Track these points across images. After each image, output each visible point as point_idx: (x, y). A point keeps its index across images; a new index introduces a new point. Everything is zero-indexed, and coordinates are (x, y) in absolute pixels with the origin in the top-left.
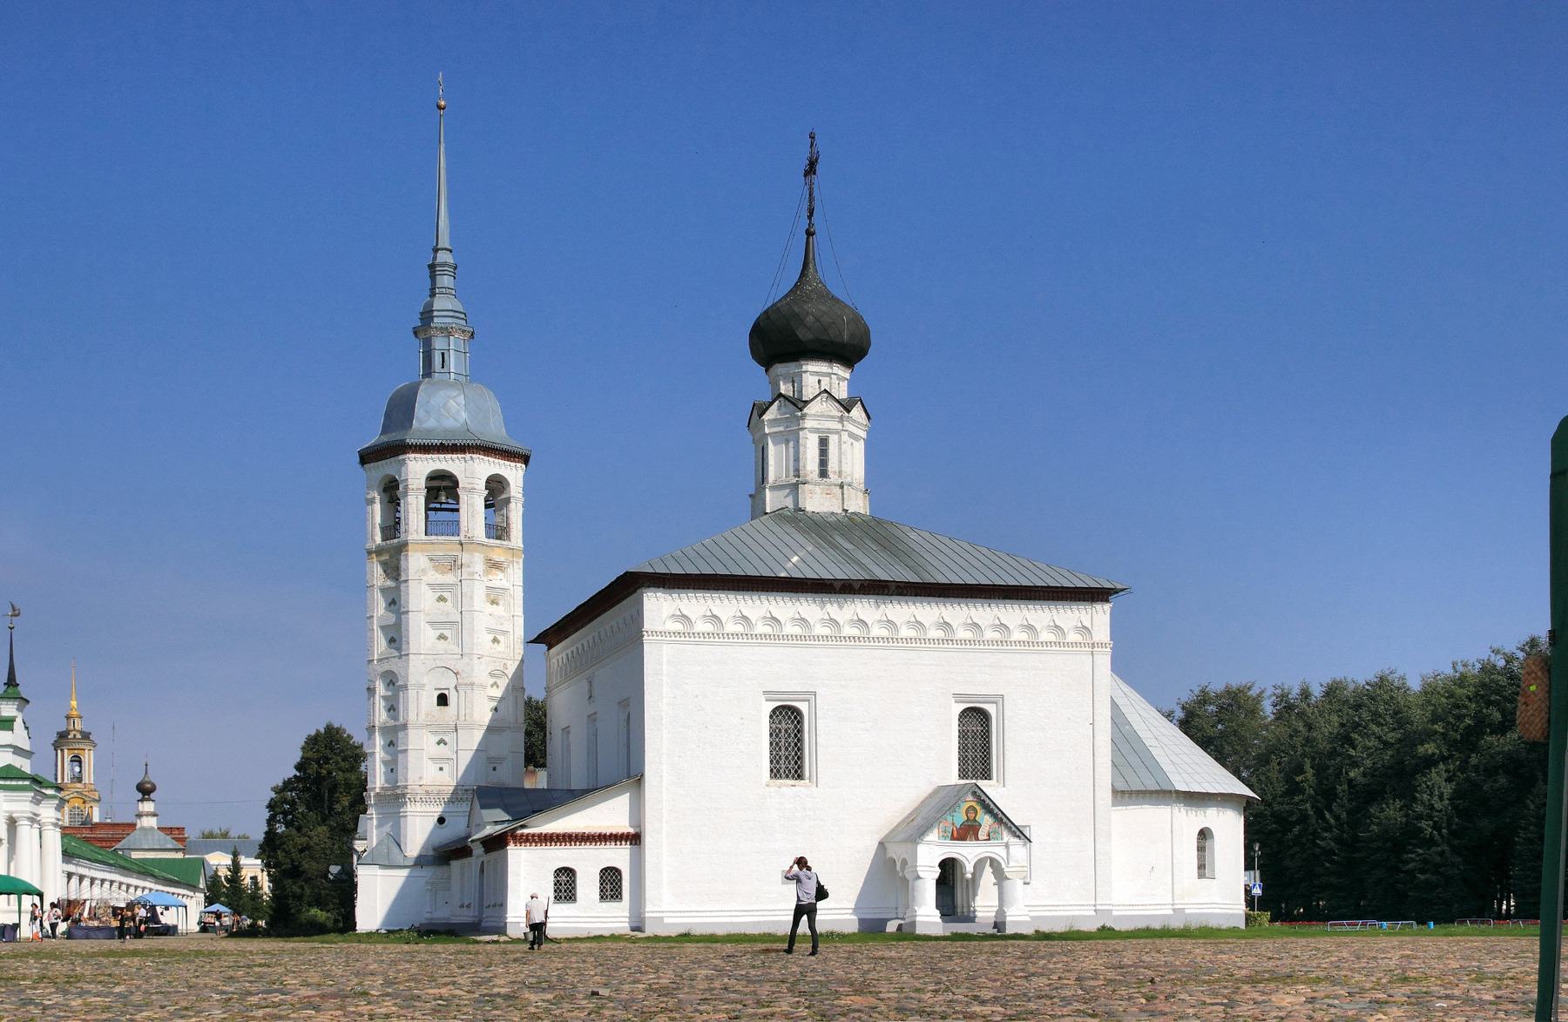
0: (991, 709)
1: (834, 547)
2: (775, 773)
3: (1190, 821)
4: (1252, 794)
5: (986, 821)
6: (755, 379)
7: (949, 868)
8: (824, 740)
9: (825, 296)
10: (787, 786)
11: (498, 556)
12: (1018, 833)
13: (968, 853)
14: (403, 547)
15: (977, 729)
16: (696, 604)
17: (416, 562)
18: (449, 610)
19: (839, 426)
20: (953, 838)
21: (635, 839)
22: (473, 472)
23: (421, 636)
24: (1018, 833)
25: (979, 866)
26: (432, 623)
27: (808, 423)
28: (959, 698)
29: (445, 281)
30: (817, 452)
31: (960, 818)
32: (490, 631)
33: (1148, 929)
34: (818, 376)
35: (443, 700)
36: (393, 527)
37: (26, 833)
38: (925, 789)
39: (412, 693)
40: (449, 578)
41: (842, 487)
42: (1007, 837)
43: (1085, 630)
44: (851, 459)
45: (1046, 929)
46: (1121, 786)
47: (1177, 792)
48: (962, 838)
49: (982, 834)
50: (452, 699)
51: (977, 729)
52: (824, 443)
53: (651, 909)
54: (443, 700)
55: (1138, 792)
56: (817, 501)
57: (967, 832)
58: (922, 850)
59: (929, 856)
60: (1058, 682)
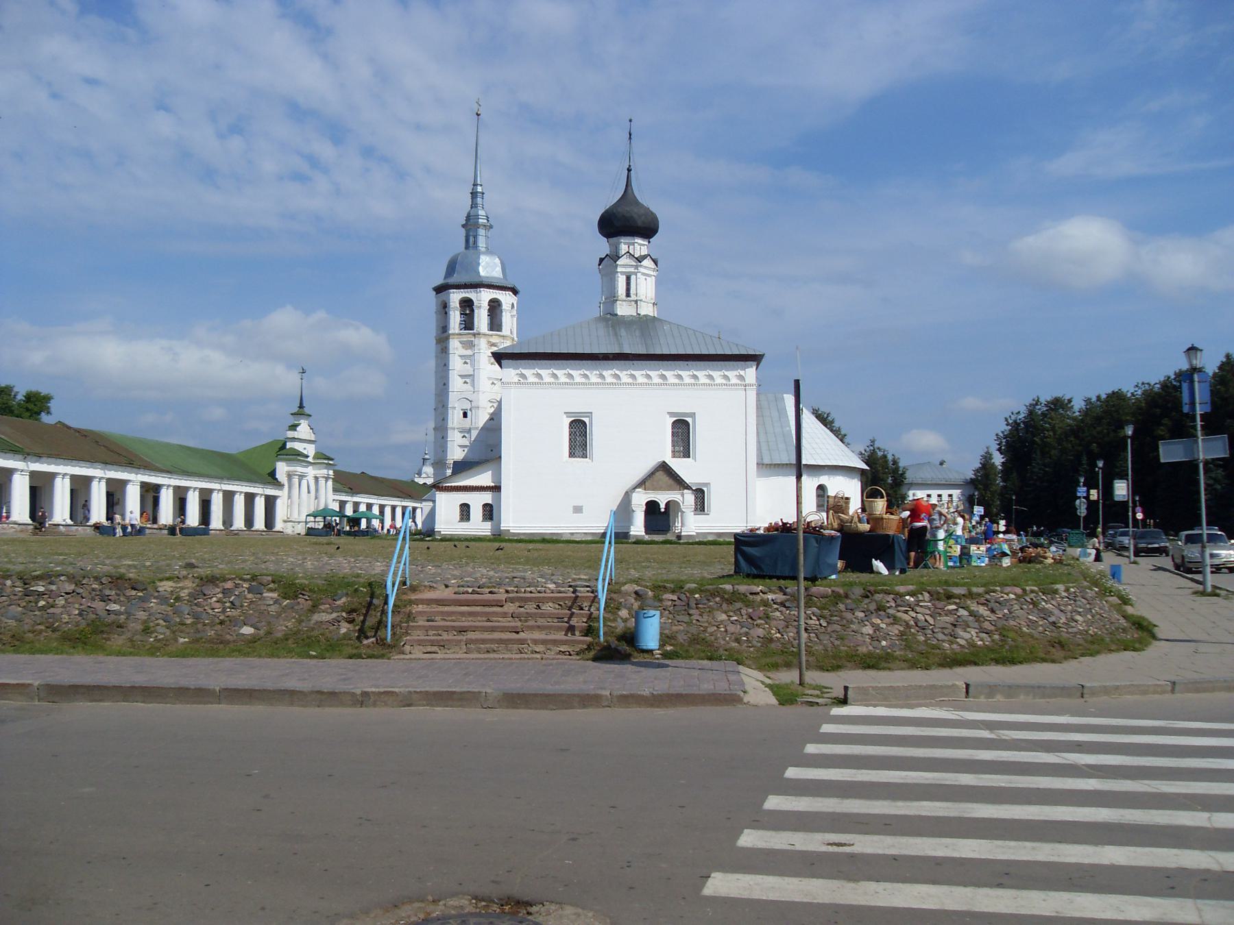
0: (689, 420)
1: (616, 334)
2: (572, 455)
4: (866, 467)
6: (603, 246)
7: (652, 507)
8: (597, 436)
9: (637, 203)
13: (662, 498)
14: (447, 338)
15: (682, 431)
17: (455, 345)
18: (468, 369)
21: (496, 489)
22: (483, 298)
23: (456, 384)
25: (668, 504)
27: (619, 269)
28: (671, 414)
29: (479, 200)
32: (489, 378)
34: (640, 246)
36: (444, 328)
37: (322, 482)
39: (450, 411)
40: (469, 352)
41: (636, 302)
43: (741, 378)
44: (646, 286)
46: (767, 461)
50: (469, 414)
51: (682, 431)
53: (504, 526)
54: (465, 415)
56: (623, 309)
59: (640, 500)
60: (725, 408)
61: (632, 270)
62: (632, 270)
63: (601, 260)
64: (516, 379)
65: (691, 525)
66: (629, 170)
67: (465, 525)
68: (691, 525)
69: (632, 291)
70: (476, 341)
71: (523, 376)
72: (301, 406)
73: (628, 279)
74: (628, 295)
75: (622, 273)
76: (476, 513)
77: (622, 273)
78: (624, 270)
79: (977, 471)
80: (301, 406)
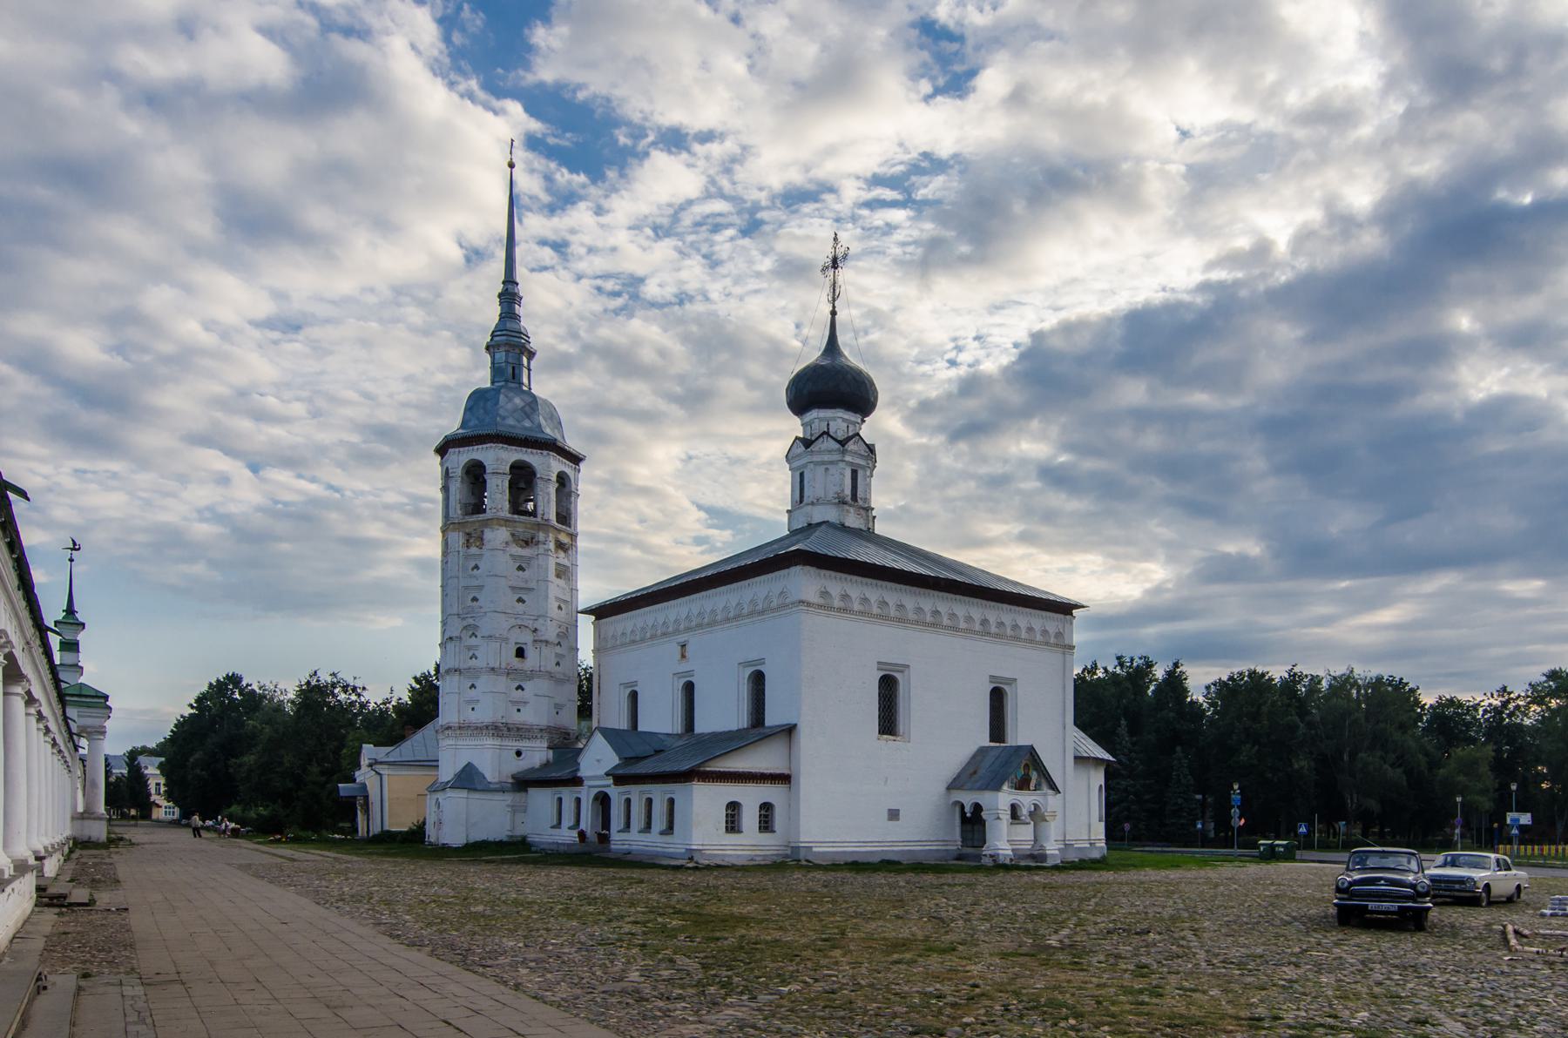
5: (1034, 775)
8: (914, 705)
10: (887, 742)
11: (564, 539)
12: (1053, 787)
24: (1053, 787)
26: (513, 588)
27: (848, 458)
28: (993, 678)
32: (557, 599)
35: (520, 653)
38: (973, 749)
42: (1045, 789)
49: (1032, 786)
50: (530, 652)
54: (520, 653)
57: (1023, 785)
61: (862, 462)
62: (862, 462)
63: (807, 443)
67: (733, 838)
69: (860, 494)
70: (541, 536)
71: (825, 594)
73: (854, 473)
76: (750, 818)
78: (848, 458)
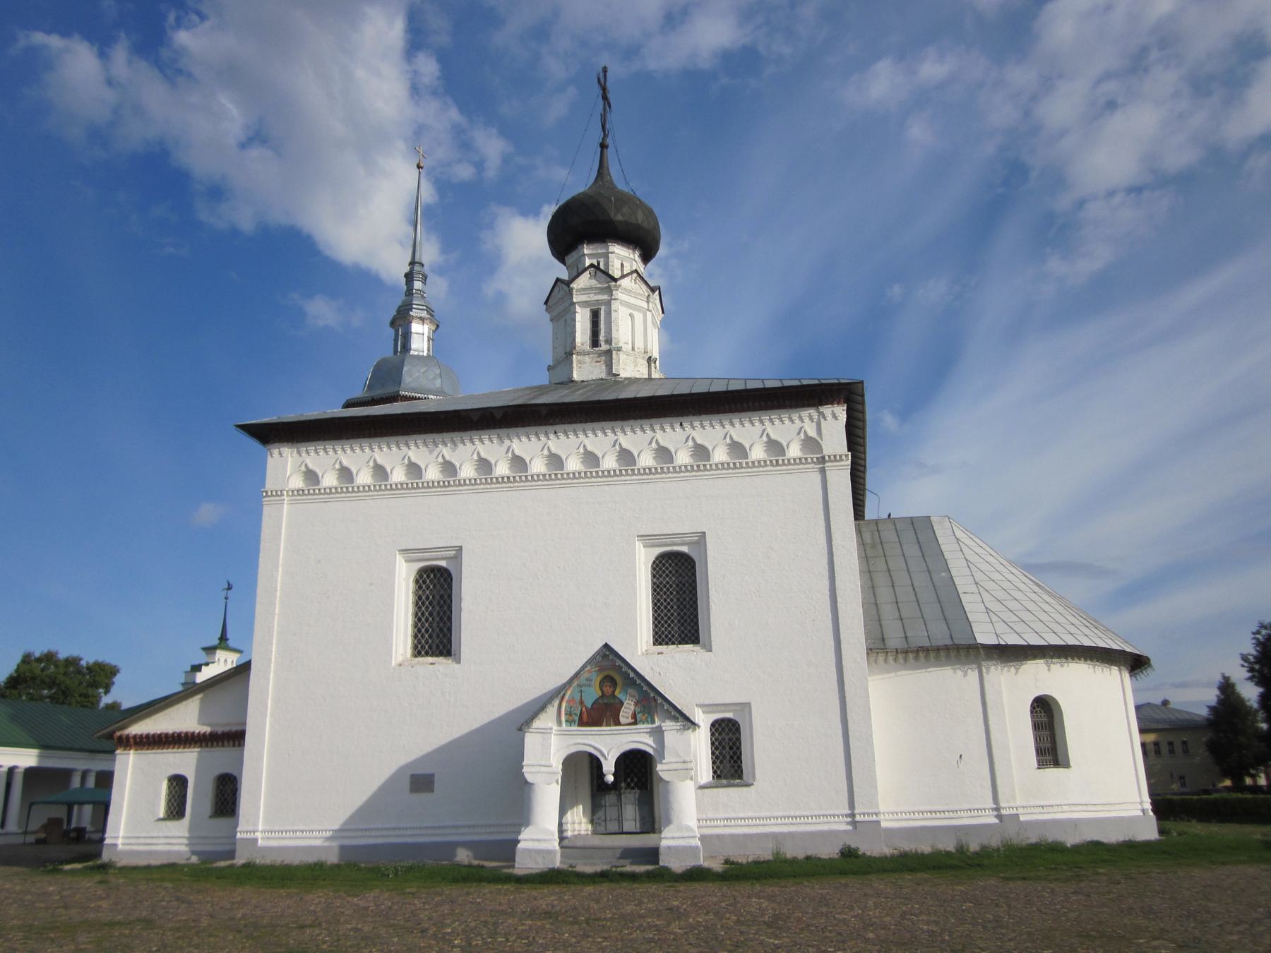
3: (1018, 686)
16: (324, 460)
19: (644, 305)
20: (582, 723)
30: (588, 325)
31: (592, 695)
33: (904, 856)
41: (609, 352)
45: (744, 855)
47: (985, 647)
48: (597, 723)
52: (595, 315)
55: (926, 650)
58: (531, 741)
64: (297, 482)
65: (695, 815)
66: (603, 146)
68: (695, 815)
72: (223, 637)
74: (595, 342)
75: (584, 304)
77: (584, 304)
78: (584, 298)
79: (1212, 709)
80: (223, 637)
